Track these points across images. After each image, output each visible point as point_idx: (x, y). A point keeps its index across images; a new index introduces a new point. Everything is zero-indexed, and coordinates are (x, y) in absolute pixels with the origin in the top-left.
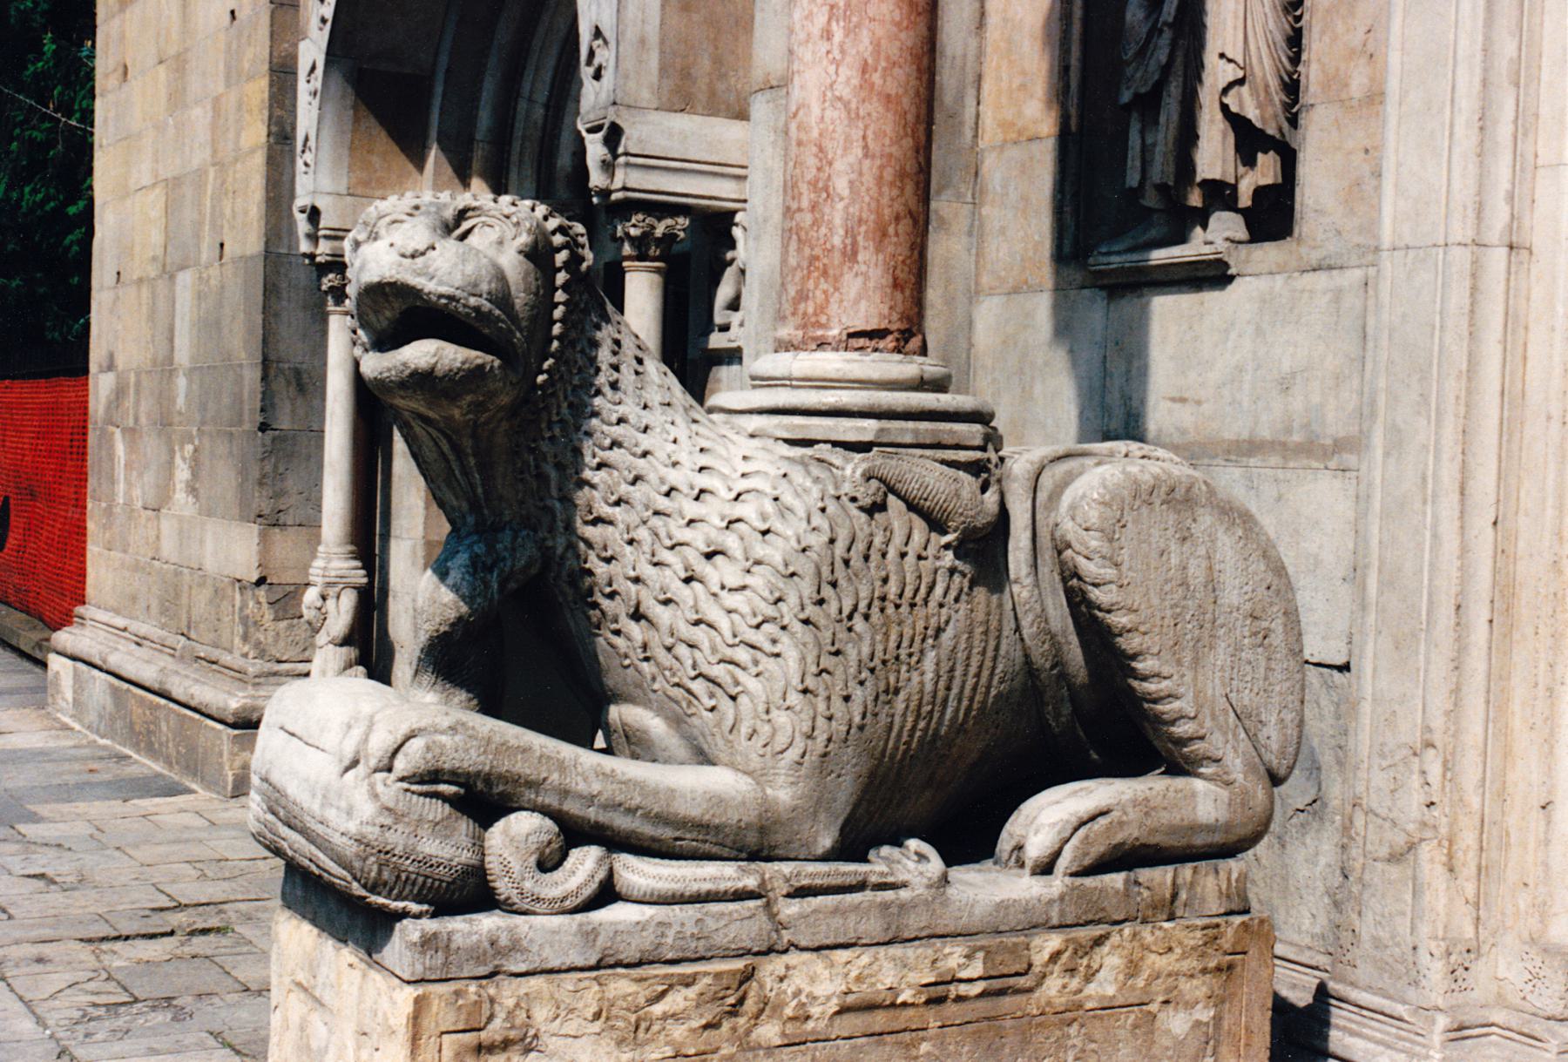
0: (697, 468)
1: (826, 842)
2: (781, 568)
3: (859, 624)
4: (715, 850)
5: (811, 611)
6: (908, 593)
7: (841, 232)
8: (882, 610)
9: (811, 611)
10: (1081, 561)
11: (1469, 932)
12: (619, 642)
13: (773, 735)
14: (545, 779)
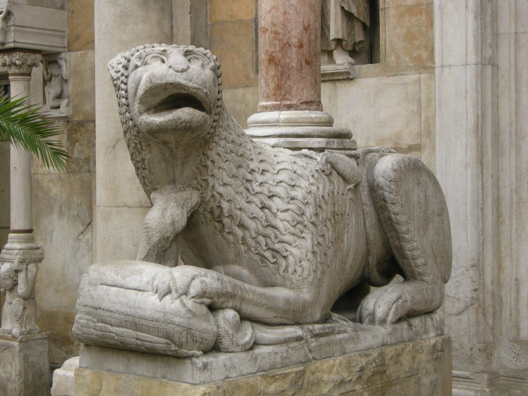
0: (259, 160)
1: (318, 316)
4: (286, 321)
7: (296, 61)
9: (314, 219)
10: (386, 194)
11: (491, 339)
12: (231, 238)
13: (303, 272)
14: (237, 294)
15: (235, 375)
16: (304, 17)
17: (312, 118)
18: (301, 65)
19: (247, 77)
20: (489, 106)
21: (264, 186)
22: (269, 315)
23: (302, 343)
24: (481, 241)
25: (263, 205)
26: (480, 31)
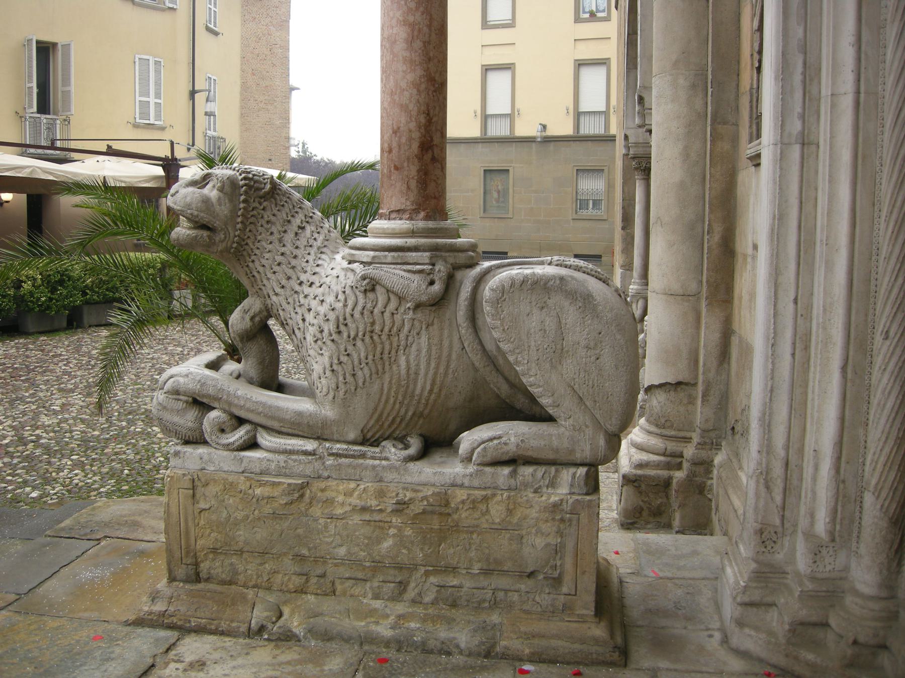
1: (352, 436)
3: (359, 343)
4: (300, 433)
6: (386, 329)
8: (371, 337)
9: (335, 336)
11: (777, 522)
15: (213, 469)
16: (393, 120)
17: (384, 229)
18: (390, 171)
20: (794, 201)
22: (275, 425)
23: (310, 458)
24: (769, 388)
26: (781, 97)
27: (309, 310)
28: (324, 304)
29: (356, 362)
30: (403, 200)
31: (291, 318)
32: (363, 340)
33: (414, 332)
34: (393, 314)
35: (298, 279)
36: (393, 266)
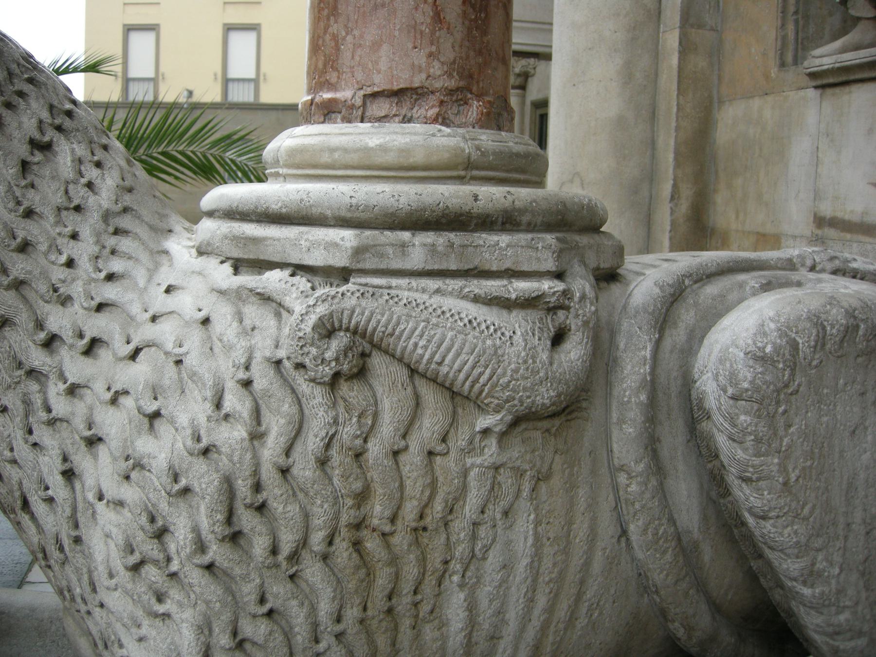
0: (94, 304)
2: (167, 480)
5: (216, 552)
6: (410, 511)
8: (357, 545)
9: (216, 552)
10: (721, 441)
19: (767, 77)
21: (81, 398)
25: (67, 466)
27: (93, 442)
28: (161, 426)
29: (301, 636)
30: (419, 57)
31: (14, 462)
32: (325, 557)
33: (495, 511)
34: (430, 453)
35: (40, 325)
36: (433, 284)
